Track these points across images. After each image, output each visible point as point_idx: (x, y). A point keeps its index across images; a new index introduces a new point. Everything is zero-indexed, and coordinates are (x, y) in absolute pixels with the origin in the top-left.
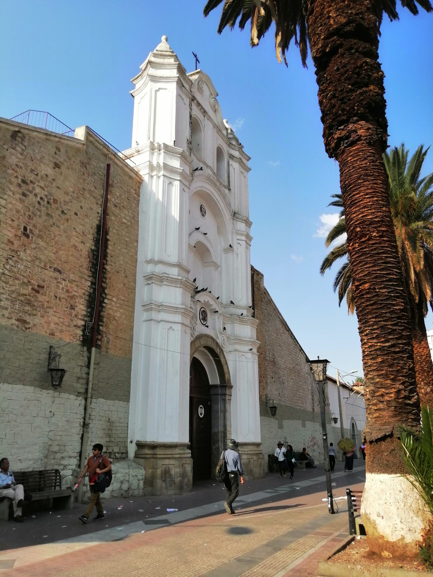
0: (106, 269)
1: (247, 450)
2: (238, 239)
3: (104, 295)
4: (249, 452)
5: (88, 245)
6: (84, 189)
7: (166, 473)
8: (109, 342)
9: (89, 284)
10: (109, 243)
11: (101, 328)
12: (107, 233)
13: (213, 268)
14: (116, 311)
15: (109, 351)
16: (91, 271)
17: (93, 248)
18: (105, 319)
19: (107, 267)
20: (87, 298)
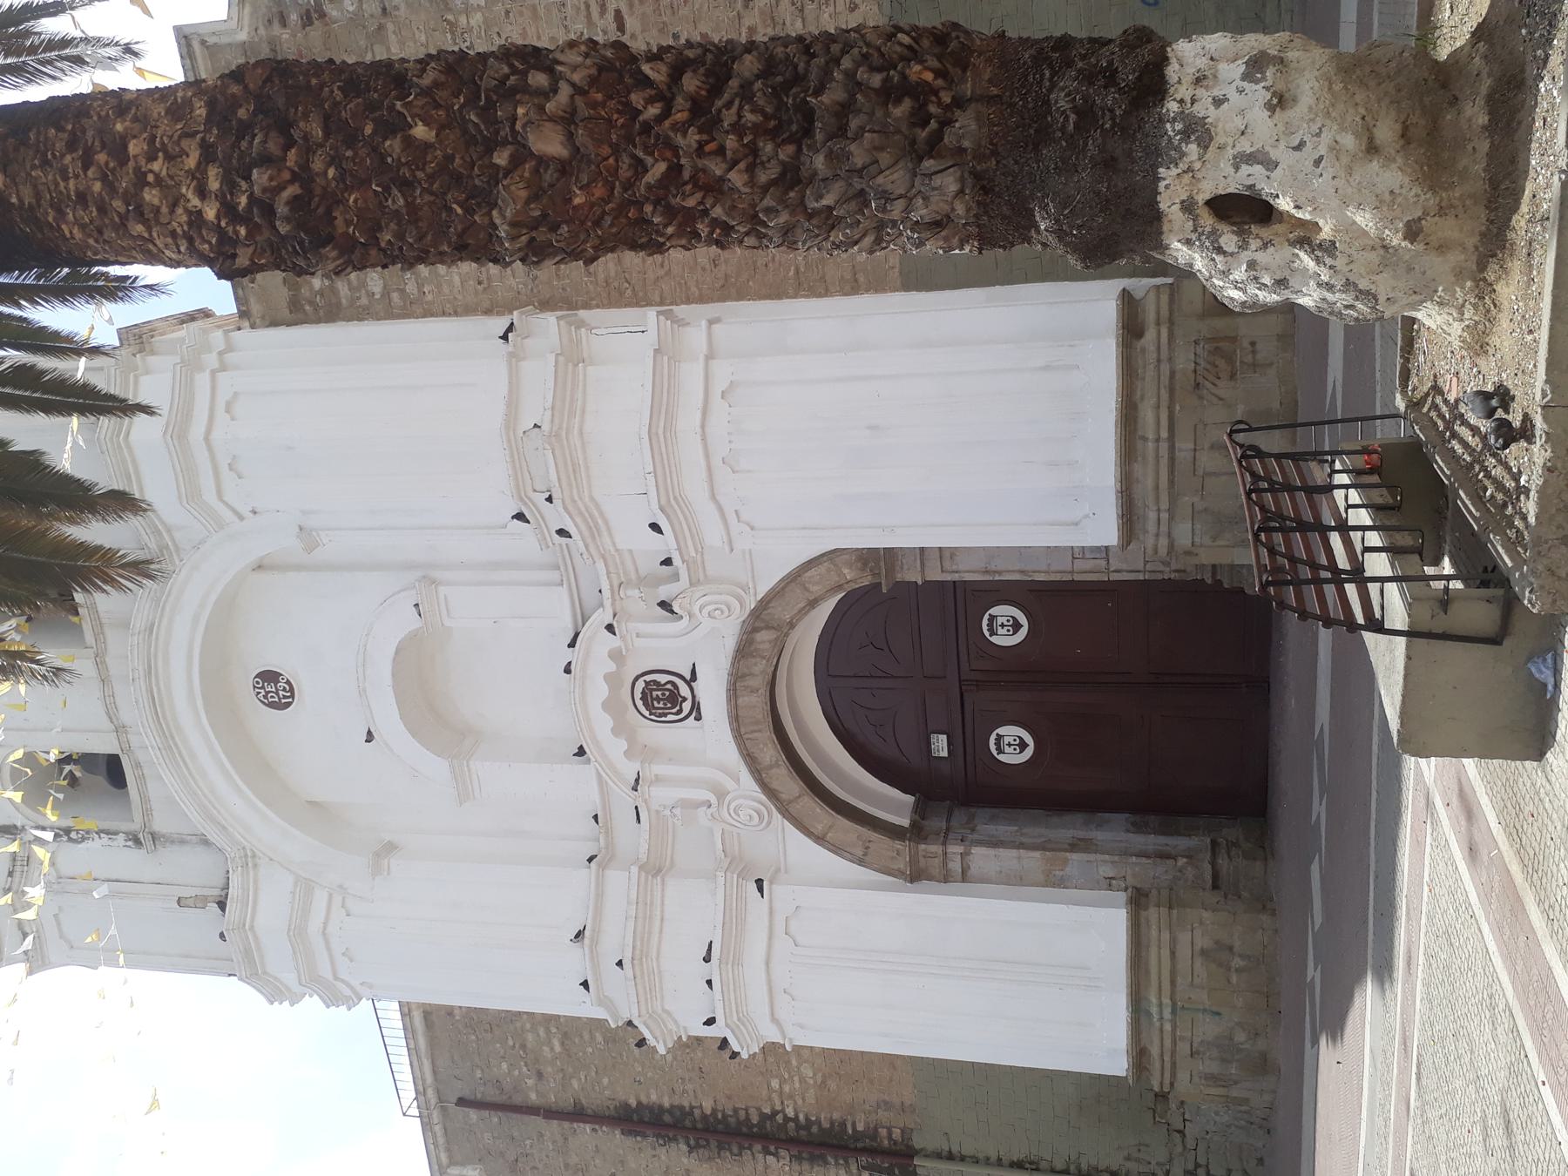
0: (714, 1111)
1: (1152, 515)
2: (241, 518)
3: (779, 1118)
4: (1164, 505)
5: (685, 1161)
6: (567, 1166)
7: (1212, 1079)
8: (886, 1103)
9: (770, 1159)
10: (644, 1100)
11: (860, 1127)
12: (627, 1105)
13: (448, 623)
14: (802, 1080)
15: (908, 1103)
16: (740, 1154)
17: (684, 1147)
18: (836, 1116)
19: (708, 1106)
20: (806, 1166)
